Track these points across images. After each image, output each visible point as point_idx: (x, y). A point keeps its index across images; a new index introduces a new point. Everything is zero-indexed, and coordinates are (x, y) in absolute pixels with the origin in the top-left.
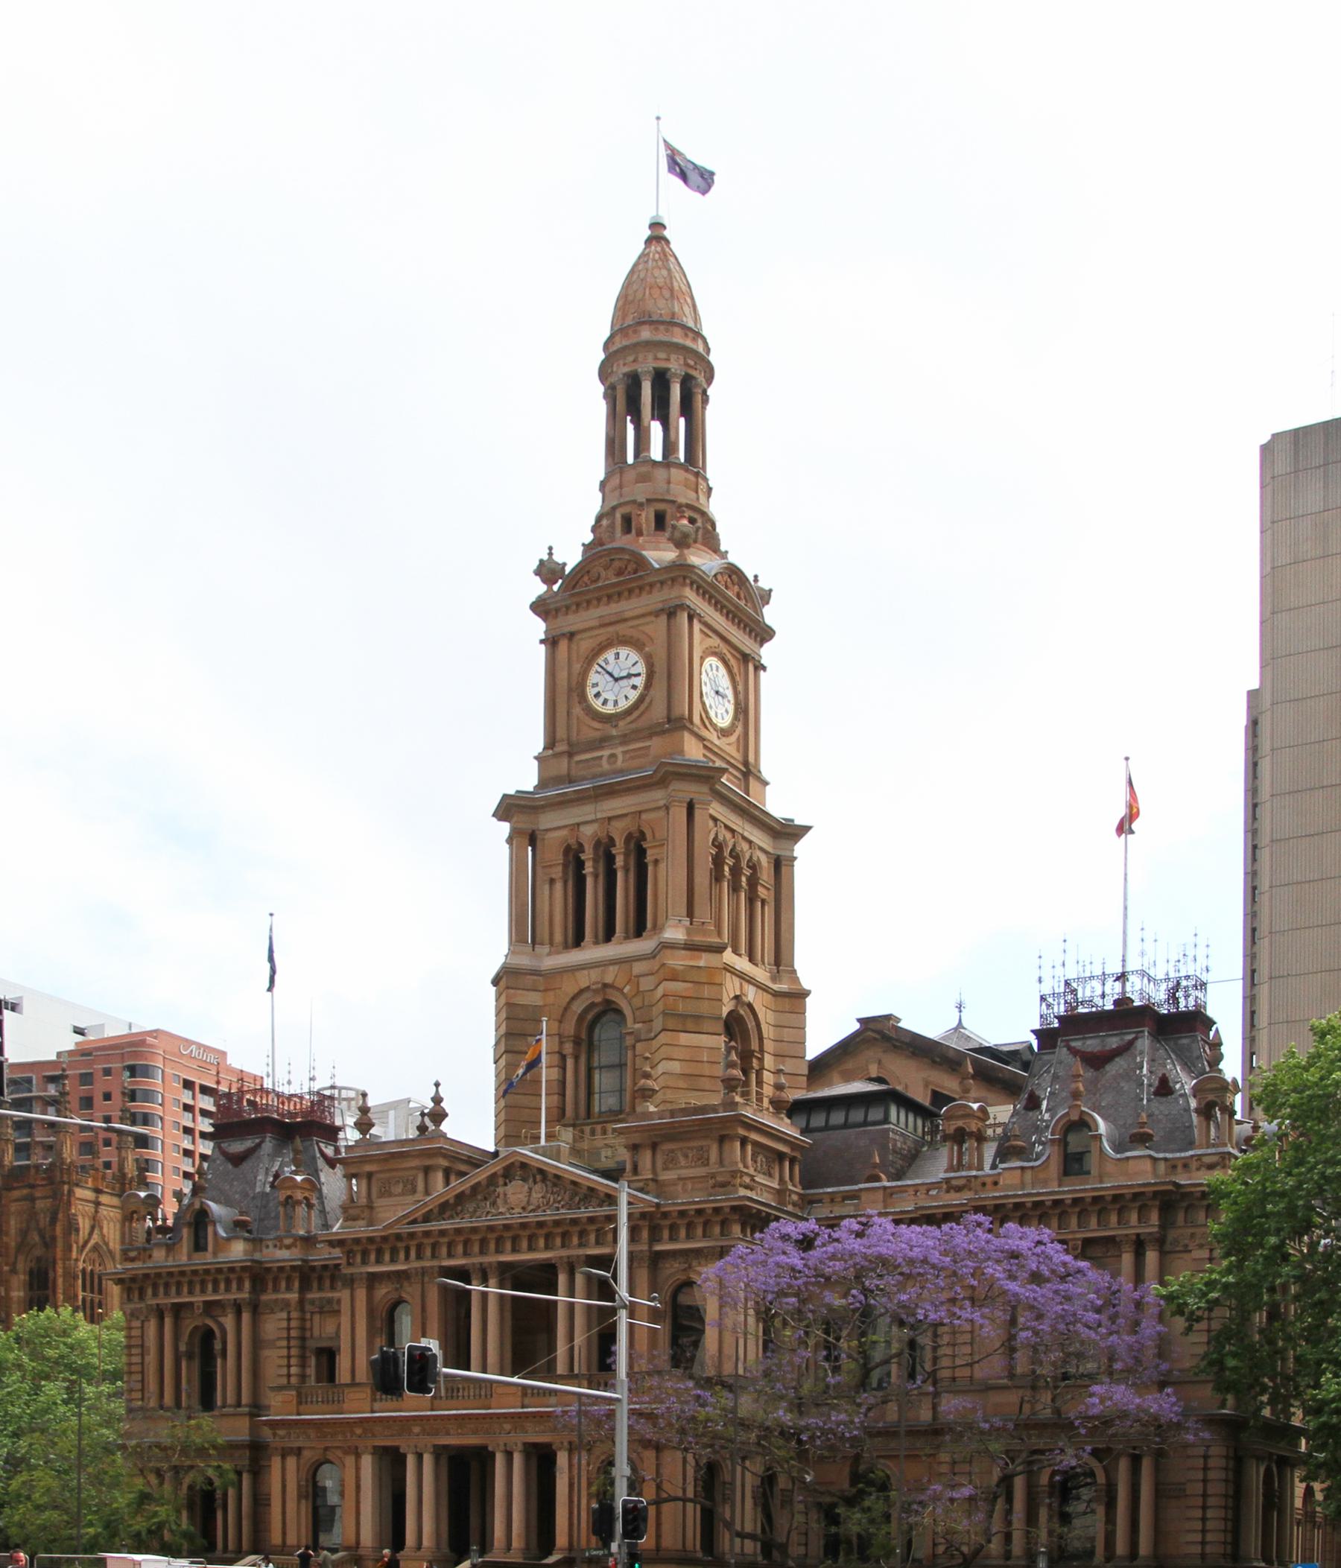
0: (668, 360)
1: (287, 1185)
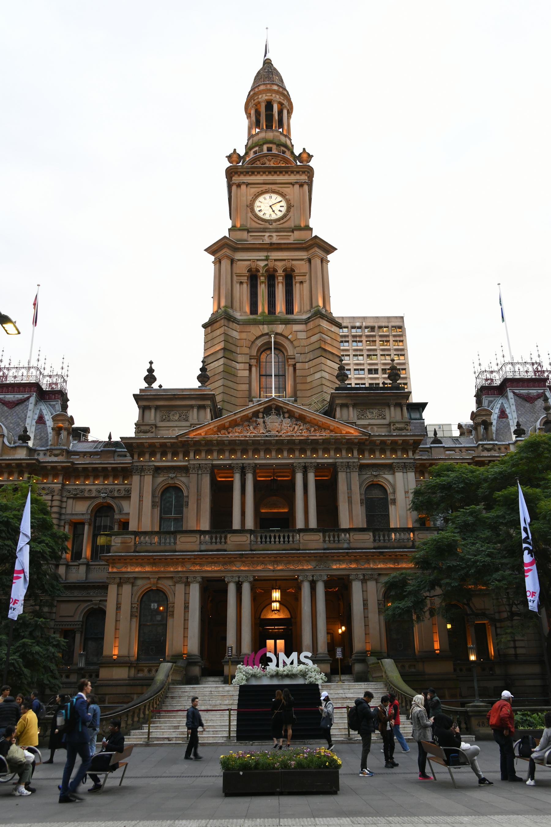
0: (271, 96)
1: (59, 418)
